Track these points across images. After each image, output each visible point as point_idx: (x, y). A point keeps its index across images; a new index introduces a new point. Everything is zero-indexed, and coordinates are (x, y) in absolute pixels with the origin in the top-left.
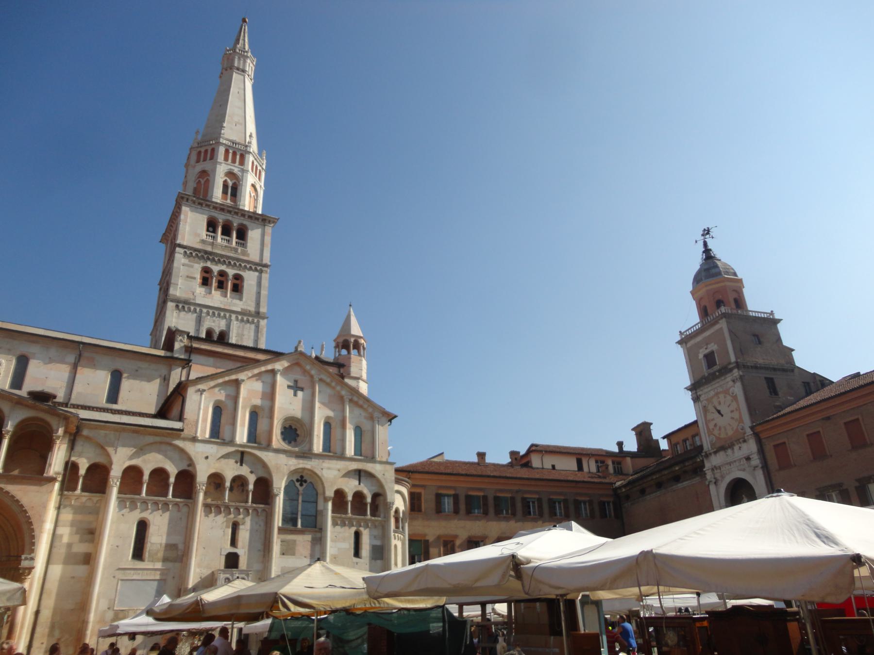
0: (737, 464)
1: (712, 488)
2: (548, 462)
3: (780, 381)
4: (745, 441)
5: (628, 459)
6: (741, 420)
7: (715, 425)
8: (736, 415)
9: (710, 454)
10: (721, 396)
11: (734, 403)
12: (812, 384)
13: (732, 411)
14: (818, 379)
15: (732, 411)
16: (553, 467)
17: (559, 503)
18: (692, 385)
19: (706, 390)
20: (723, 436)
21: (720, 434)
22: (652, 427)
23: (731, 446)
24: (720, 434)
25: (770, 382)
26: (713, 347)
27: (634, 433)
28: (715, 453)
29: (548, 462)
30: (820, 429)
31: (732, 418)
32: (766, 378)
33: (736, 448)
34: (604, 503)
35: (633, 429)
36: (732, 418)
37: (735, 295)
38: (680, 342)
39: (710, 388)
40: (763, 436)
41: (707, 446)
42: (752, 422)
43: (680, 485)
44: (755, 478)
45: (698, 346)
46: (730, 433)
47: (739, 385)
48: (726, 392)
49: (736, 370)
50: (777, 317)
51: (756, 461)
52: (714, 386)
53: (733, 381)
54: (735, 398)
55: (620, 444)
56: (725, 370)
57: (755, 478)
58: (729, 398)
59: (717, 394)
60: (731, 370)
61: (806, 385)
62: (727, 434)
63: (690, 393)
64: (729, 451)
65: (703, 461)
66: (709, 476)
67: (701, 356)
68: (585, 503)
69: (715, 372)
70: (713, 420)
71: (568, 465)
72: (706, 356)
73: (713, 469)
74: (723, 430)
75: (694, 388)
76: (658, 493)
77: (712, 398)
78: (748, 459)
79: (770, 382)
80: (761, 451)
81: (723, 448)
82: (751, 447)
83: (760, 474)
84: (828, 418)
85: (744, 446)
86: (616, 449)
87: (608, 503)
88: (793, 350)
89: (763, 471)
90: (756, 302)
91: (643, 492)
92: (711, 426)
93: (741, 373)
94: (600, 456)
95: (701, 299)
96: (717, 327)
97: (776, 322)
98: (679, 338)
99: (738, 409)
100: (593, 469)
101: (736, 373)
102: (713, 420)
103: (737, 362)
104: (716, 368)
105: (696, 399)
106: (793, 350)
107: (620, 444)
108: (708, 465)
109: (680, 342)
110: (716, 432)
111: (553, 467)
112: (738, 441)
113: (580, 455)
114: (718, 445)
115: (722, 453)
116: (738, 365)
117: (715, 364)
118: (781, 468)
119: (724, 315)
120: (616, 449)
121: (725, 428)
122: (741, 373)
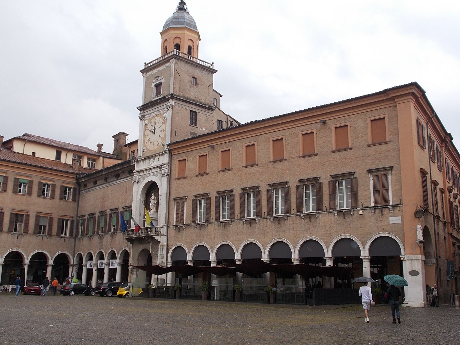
0: (154, 170)
2: (29, 150)
3: (202, 115)
4: (162, 155)
5: (101, 158)
7: (149, 140)
8: (162, 134)
9: (140, 160)
10: (158, 118)
11: (164, 125)
12: (224, 123)
13: (161, 131)
14: (229, 119)
15: (161, 131)
16: (34, 154)
17: (25, 184)
18: (143, 106)
19: (150, 112)
21: (150, 147)
22: (127, 137)
23: (154, 156)
24: (150, 147)
25: (194, 114)
27: (114, 139)
28: (143, 160)
29: (29, 150)
30: (207, 154)
31: (160, 136)
32: (191, 111)
33: (156, 158)
34: (66, 188)
35: (113, 137)
36: (160, 136)
37: (190, 44)
38: (142, 71)
39: (152, 111)
40: (174, 152)
42: (171, 141)
44: (161, 182)
46: (156, 147)
47: (170, 112)
49: (170, 101)
50: (215, 68)
51: (165, 171)
53: (167, 109)
55: (100, 146)
56: (164, 100)
57: (161, 182)
58: (162, 121)
60: (168, 100)
61: (220, 122)
62: (154, 148)
63: (139, 112)
65: (134, 166)
67: (153, 85)
68: (48, 185)
71: (51, 155)
72: (156, 86)
73: (140, 171)
75: (143, 108)
77: (152, 118)
78: (161, 167)
79: (194, 114)
80: (170, 164)
81: (148, 158)
83: (165, 179)
84: (213, 147)
85: (161, 157)
86: (96, 149)
87: (70, 189)
88: (221, 96)
89: (168, 178)
90: (204, 54)
91: (95, 183)
92: (146, 141)
93: (173, 104)
94: (79, 153)
95: (166, 40)
96: (167, 65)
97: (214, 71)
98: (143, 68)
99: (165, 130)
100: (70, 162)
101: (171, 102)
102: (148, 135)
103: (172, 94)
105: (142, 118)
106: (221, 96)
107: (100, 146)
108: (137, 169)
109: (142, 71)
110: (148, 145)
111: (34, 154)
113: (60, 149)
114: (146, 155)
115: (147, 161)
116: (173, 97)
119: (174, 56)
120: (96, 149)
121: (154, 144)
122: (173, 104)
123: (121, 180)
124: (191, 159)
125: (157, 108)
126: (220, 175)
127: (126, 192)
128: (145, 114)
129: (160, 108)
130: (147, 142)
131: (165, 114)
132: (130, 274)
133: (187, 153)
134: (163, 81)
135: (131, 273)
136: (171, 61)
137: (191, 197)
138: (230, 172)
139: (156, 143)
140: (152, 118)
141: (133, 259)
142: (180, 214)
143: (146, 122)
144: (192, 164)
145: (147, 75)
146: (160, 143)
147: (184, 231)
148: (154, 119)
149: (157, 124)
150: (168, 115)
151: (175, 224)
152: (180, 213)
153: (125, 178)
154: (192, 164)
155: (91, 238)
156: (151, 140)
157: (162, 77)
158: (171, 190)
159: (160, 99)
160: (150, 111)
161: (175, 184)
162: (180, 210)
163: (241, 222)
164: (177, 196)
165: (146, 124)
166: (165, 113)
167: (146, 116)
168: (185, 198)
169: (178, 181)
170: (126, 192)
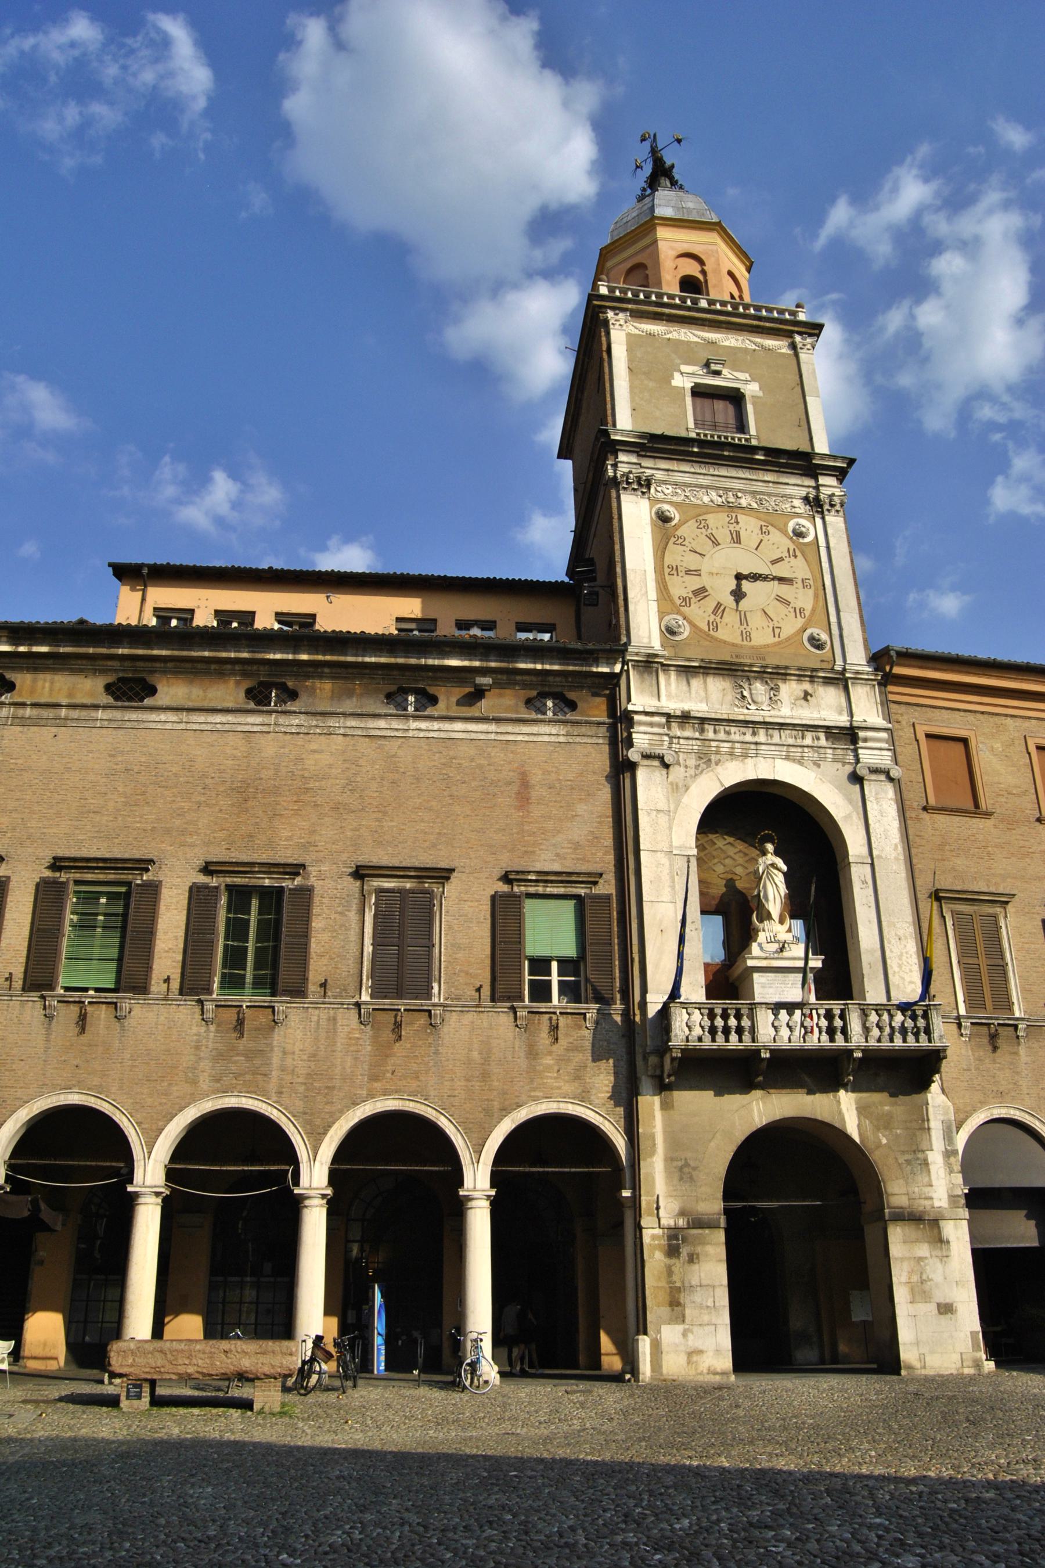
0: (787, 737)
1: (649, 787)
7: (701, 592)
19: (687, 479)
20: (722, 634)
23: (775, 674)
28: (687, 671)
33: (789, 689)
46: (761, 637)
47: (836, 522)
48: (772, 520)
58: (779, 543)
62: (748, 636)
64: (759, 688)
66: (642, 739)
67: (683, 381)
69: (755, 449)
70: (697, 573)
72: (699, 392)
77: (706, 509)
82: (866, 707)
108: (639, 698)
112: (810, 675)
123: (459, 726)
124: (998, 746)
127: (523, 797)
129: (760, 487)
132: (655, 1260)
134: (751, 390)
135: (673, 1251)
136: (798, 338)
139: (756, 621)
141: (682, 1171)
142: (984, 970)
147: (1022, 1050)
151: (962, 1011)
152: (983, 962)
155: (101, 1016)
158: (913, 851)
159: (769, 451)
160: (684, 472)
162: (981, 949)
165: (663, 518)
166: (798, 515)
168: (1003, 901)
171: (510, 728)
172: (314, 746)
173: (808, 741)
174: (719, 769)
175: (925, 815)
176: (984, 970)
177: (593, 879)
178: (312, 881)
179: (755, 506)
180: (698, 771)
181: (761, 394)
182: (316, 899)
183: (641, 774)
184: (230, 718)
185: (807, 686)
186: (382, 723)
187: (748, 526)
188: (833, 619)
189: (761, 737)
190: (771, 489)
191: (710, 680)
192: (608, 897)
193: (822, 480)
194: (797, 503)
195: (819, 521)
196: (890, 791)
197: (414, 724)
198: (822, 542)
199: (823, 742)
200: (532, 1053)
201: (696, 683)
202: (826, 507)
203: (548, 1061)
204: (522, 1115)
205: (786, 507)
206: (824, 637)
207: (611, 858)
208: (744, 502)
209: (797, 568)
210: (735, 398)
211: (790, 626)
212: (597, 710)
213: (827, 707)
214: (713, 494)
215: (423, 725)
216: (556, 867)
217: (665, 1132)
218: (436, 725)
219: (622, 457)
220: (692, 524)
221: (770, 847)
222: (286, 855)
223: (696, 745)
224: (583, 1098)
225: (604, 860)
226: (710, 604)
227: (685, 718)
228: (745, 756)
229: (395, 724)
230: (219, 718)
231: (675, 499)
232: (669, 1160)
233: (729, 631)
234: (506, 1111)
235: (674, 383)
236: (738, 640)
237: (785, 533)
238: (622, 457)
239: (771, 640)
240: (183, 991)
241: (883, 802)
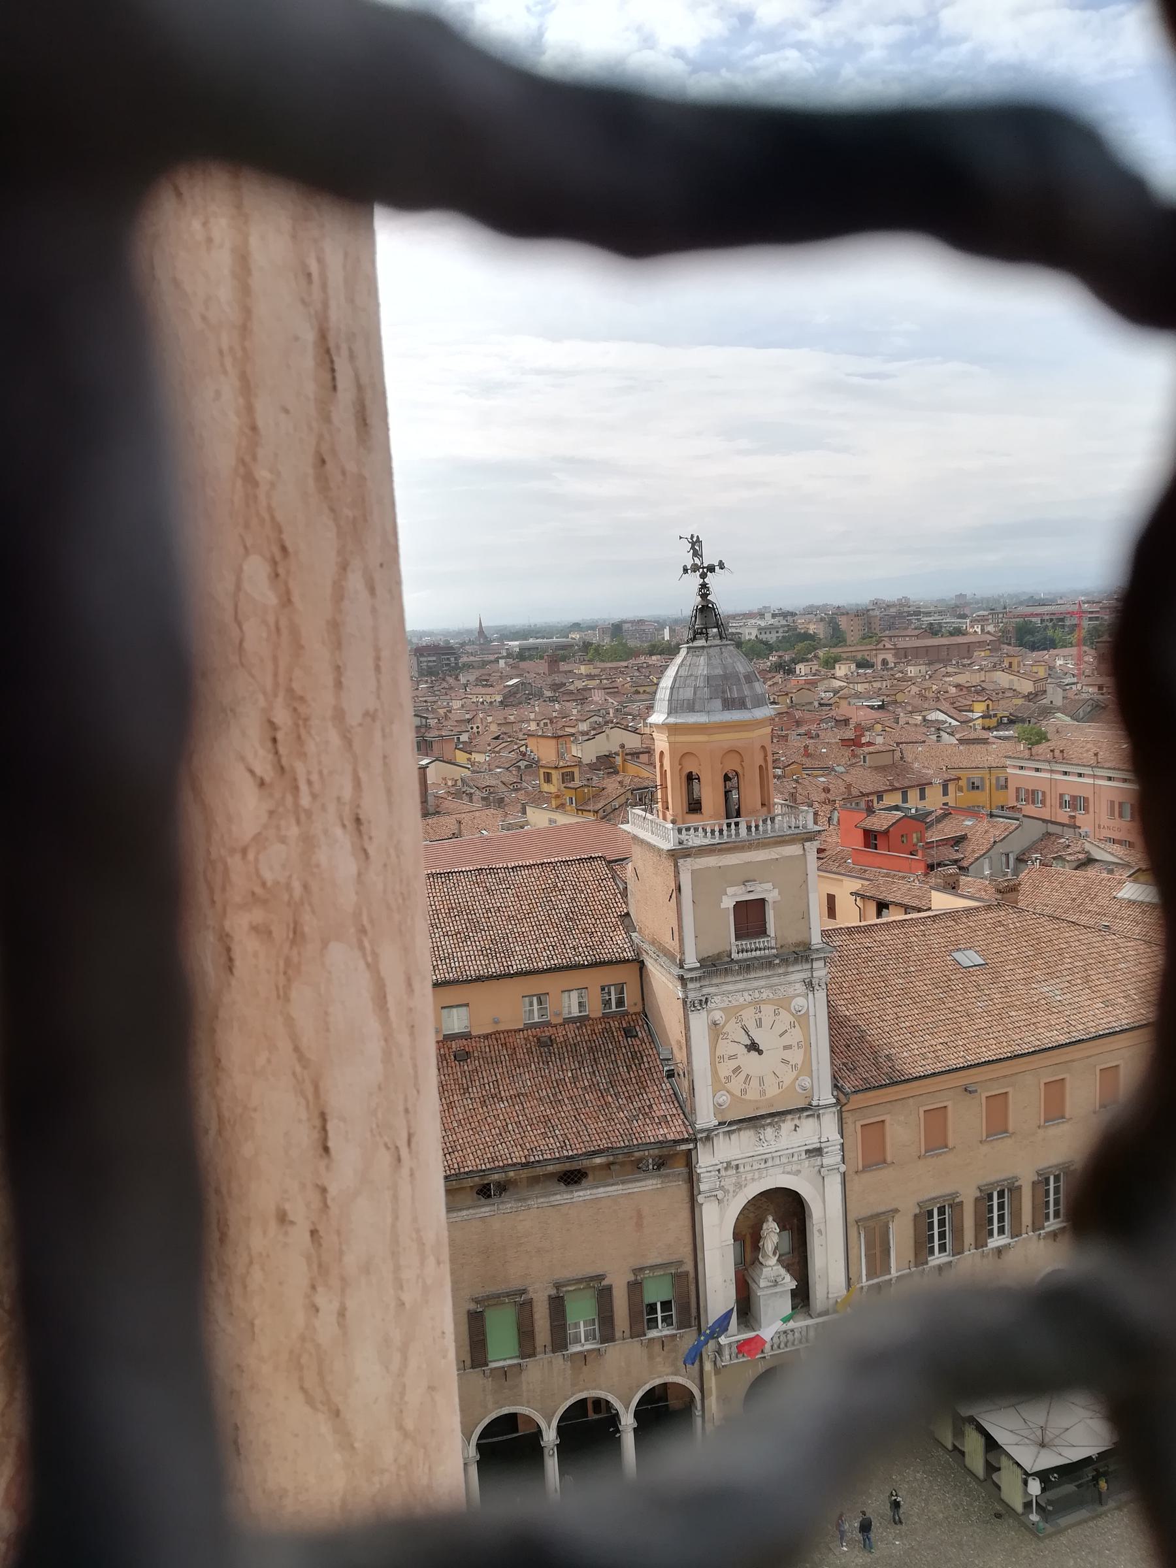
6: (807, 1068)
7: (737, 1070)
8: (797, 1056)
10: (768, 1010)
13: (786, 1048)
15: (786, 1048)
19: (730, 987)
26: (767, 891)
31: (785, 1061)
33: (787, 1125)
36: (785, 1061)
39: (741, 986)
41: (705, 1118)
43: (581, 1194)
45: (725, 876)
46: (772, 1091)
48: (783, 1004)
51: (832, 1158)
52: (756, 984)
53: (810, 985)
54: (801, 1019)
58: (786, 1017)
59: (757, 1004)
60: (807, 959)
64: (769, 1131)
67: (728, 903)
72: (739, 906)
74: (754, 1083)
76: (485, 1211)
77: (742, 1007)
78: (817, 1152)
82: (828, 1128)
99: (806, 1045)
104: (761, 942)
110: (736, 1085)
117: (763, 932)
118: (867, 1168)
121: (761, 1081)
123: (601, 1190)
124: (902, 1118)
125: (759, 981)
126: (985, 1149)
127: (639, 1225)
128: (705, 991)
129: (775, 980)
130: (728, 1079)
131: (800, 1002)
133: (888, 1105)
137: (909, 1208)
138: (1009, 1141)
139: (770, 1081)
140: (742, 1007)
143: (718, 1016)
144: (903, 1130)
145: (696, 867)
146: (787, 1082)
148: (751, 1010)
149: (767, 1022)
150: (817, 1006)
152: (878, 1251)
153: (623, 1183)
154: (903, 1130)
156: (745, 1071)
157: (769, 886)
161: (856, 1184)
163: (1035, 1238)
164: (866, 1212)
165: (715, 1024)
166: (799, 995)
167: (717, 999)
169: (867, 1178)
170: (639, 1225)
171: (630, 1186)
172: (521, 1218)
173: (795, 1158)
174: (745, 1190)
175: (856, 1177)
176: (878, 1254)
177: (680, 1263)
178: (531, 1295)
179: (771, 996)
180: (735, 1193)
181: (779, 898)
182: (534, 1304)
183: (704, 1207)
184: (471, 1211)
185: (797, 1122)
186: (558, 1197)
187: (768, 1010)
188: (814, 1068)
189: (770, 1163)
190: (782, 979)
191: (742, 1133)
192: (687, 1274)
193: (816, 965)
194: (798, 986)
195: (811, 995)
196: (838, 1178)
197: (576, 1194)
198: (811, 1012)
199: (804, 1156)
200: (651, 1357)
201: (733, 1137)
202: (817, 987)
203: (659, 1359)
204: (647, 1387)
205: (791, 992)
206: (806, 1082)
207: (689, 1249)
208: (764, 996)
209: (796, 1035)
210: (762, 902)
211: (788, 1077)
212: (682, 1169)
213: (808, 1132)
214: (746, 994)
215: (581, 1193)
216: (659, 1261)
217: (717, 1387)
218: (589, 1192)
219: (690, 986)
220: (734, 1020)
221: (770, 1218)
222: (516, 1285)
223: (734, 1180)
224: (675, 1374)
225: (685, 1251)
226: (742, 1076)
227: (728, 1165)
228: (760, 1178)
229: (565, 1196)
230: (464, 1213)
231: (722, 1005)
232: (718, 1398)
233: (752, 1095)
234: (639, 1387)
235: (723, 906)
236: (758, 1098)
237: (789, 1011)
238: (690, 986)
239: (779, 1091)
240: (473, 1367)
241: (834, 1186)
